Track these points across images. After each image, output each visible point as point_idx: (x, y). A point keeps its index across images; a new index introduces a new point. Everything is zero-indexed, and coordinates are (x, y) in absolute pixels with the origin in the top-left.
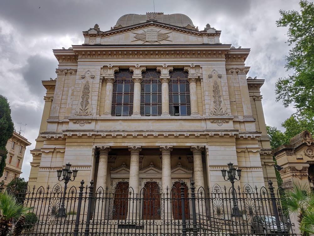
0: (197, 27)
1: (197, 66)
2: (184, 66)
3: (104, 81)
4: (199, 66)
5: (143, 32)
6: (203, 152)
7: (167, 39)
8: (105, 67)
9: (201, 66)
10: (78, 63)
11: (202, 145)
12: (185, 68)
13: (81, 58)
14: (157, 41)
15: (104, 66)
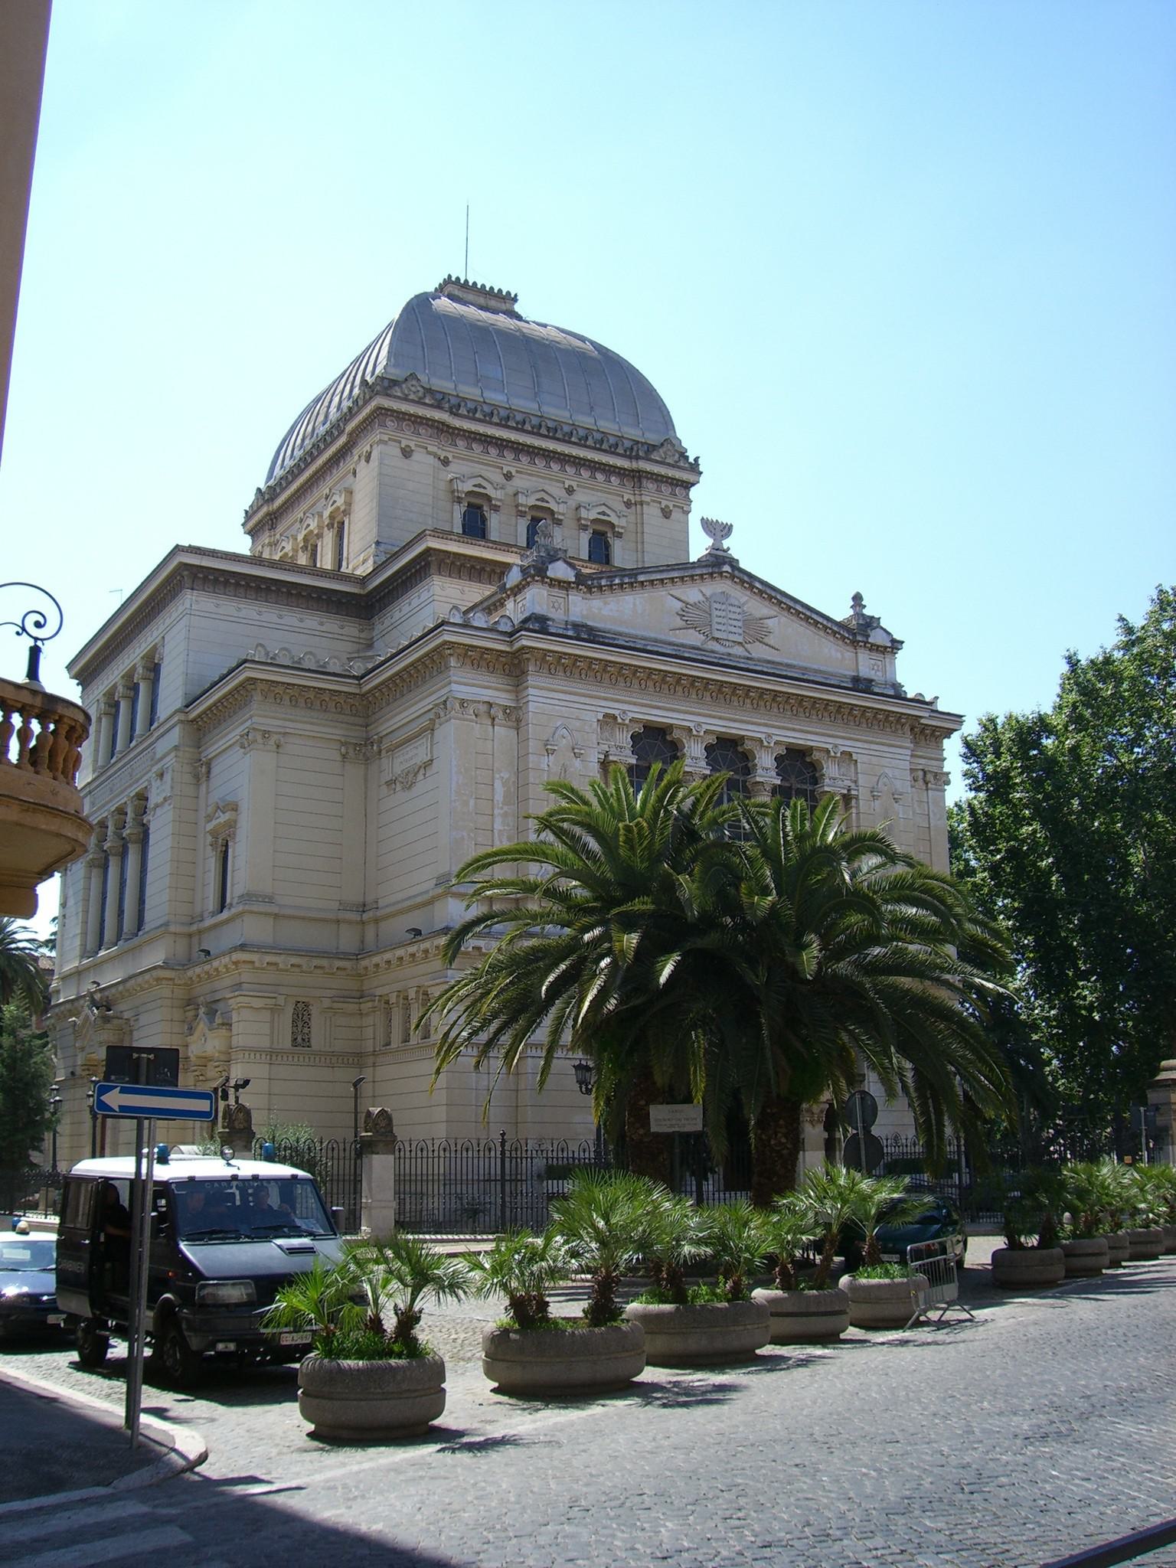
0: (696, 459)
4: (850, 754)
5: (701, 598)
7: (766, 640)
8: (609, 721)
12: (816, 755)
15: (606, 716)
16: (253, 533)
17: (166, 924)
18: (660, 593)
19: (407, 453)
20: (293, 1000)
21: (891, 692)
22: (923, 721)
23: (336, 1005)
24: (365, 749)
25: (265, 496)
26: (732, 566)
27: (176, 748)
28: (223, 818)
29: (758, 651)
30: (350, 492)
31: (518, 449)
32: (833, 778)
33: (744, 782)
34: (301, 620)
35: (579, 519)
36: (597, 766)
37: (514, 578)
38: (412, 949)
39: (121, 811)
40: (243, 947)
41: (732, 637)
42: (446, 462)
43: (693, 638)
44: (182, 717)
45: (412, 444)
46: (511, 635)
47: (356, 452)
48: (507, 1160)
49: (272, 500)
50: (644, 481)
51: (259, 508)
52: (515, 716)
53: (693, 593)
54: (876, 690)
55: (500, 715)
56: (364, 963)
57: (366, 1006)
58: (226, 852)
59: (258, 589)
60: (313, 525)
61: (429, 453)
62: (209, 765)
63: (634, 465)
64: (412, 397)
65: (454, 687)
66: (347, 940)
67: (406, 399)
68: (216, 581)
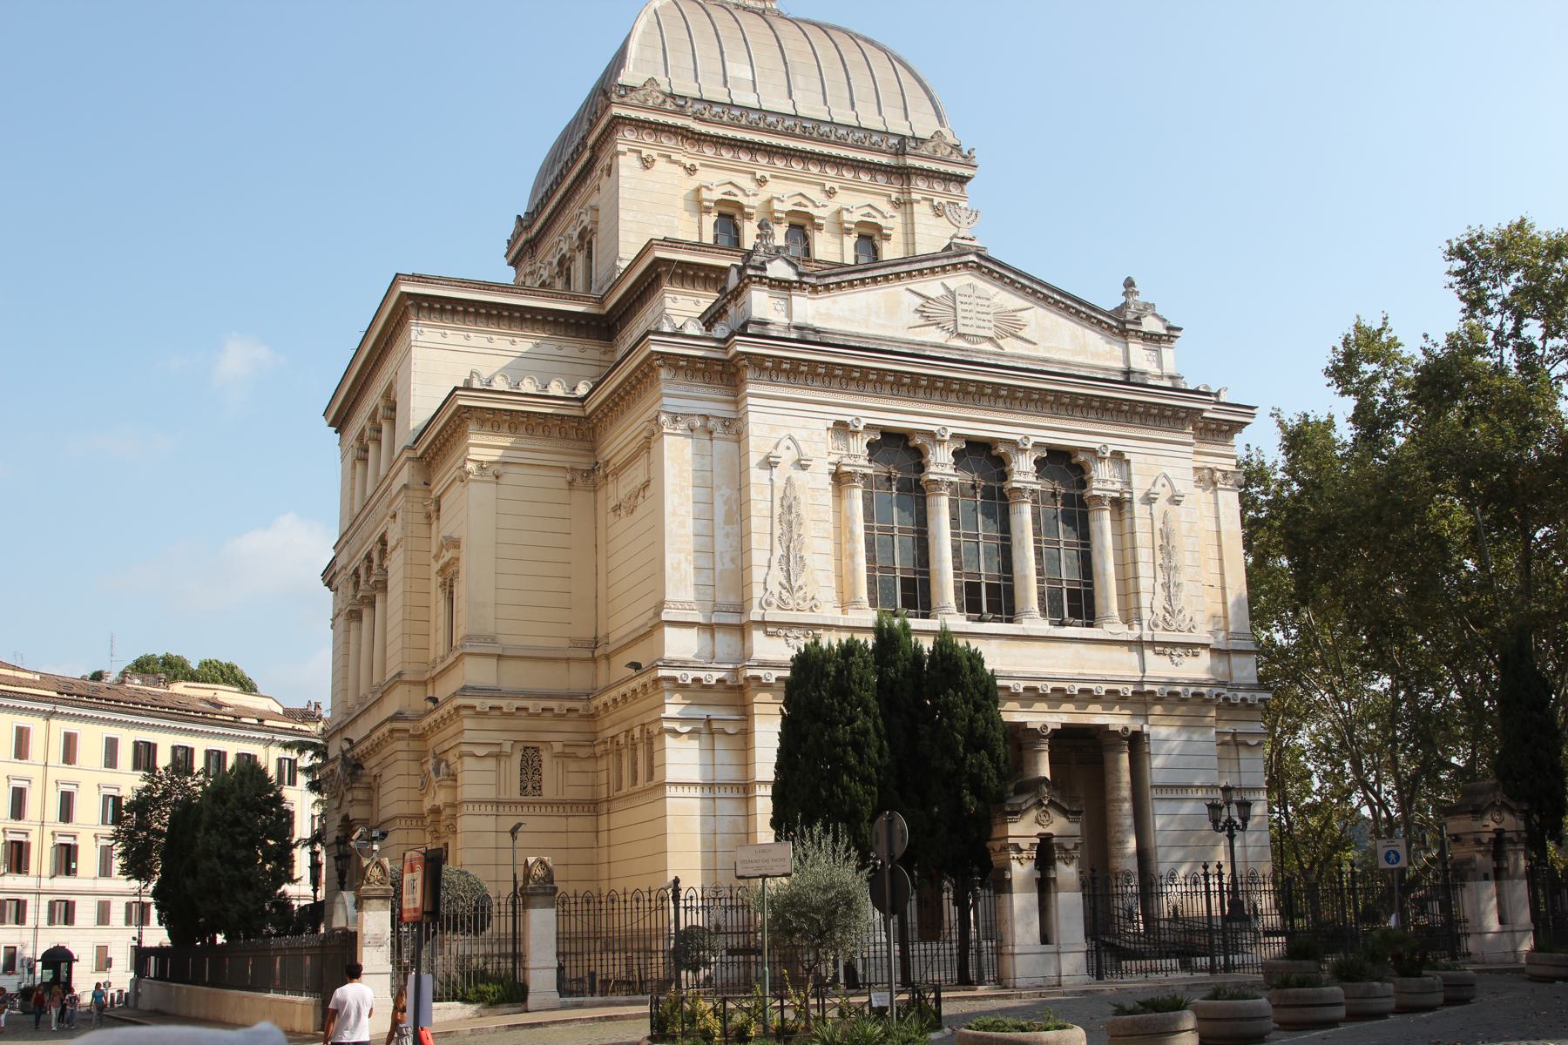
1: (1118, 456)
2: (1076, 450)
3: (840, 479)
6: (1136, 742)
7: (1020, 333)
8: (842, 429)
9: (1127, 456)
10: (750, 400)
11: (1134, 725)
12: (1082, 458)
13: (757, 381)
14: (990, 339)
15: (837, 423)
16: (514, 263)
17: (400, 674)
18: (898, 290)
19: (647, 163)
20: (520, 746)
21: (1168, 384)
22: (1206, 414)
23: (568, 750)
24: (591, 476)
25: (523, 223)
26: (979, 256)
27: (405, 486)
28: (447, 555)
29: (1011, 346)
30: (596, 209)
31: (771, 151)
32: (1104, 480)
33: (1001, 489)
34: (560, 348)
35: (841, 224)
36: (829, 479)
37: (733, 281)
38: (633, 684)
39: (369, 557)
40: (464, 691)
41: (981, 332)
42: (691, 170)
43: (933, 335)
44: (410, 454)
45: (654, 154)
46: (726, 340)
47: (599, 166)
48: (682, 911)
49: (530, 227)
50: (913, 178)
51: (520, 234)
52: (735, 428)
53: (932, 287)
54: (1151, 382)
55: (719, 428)
56: (595, 703)
57: (599, 749)
58: (451, 593)
59: (489, 316)
60: (565, 247)
61: (675, 162)
62: (438, 501)
63: (901, 162)
64: (650, 103)
65: (665, 400)
66: (577, 678)
67: (643, 107)
68: (442, 311)
